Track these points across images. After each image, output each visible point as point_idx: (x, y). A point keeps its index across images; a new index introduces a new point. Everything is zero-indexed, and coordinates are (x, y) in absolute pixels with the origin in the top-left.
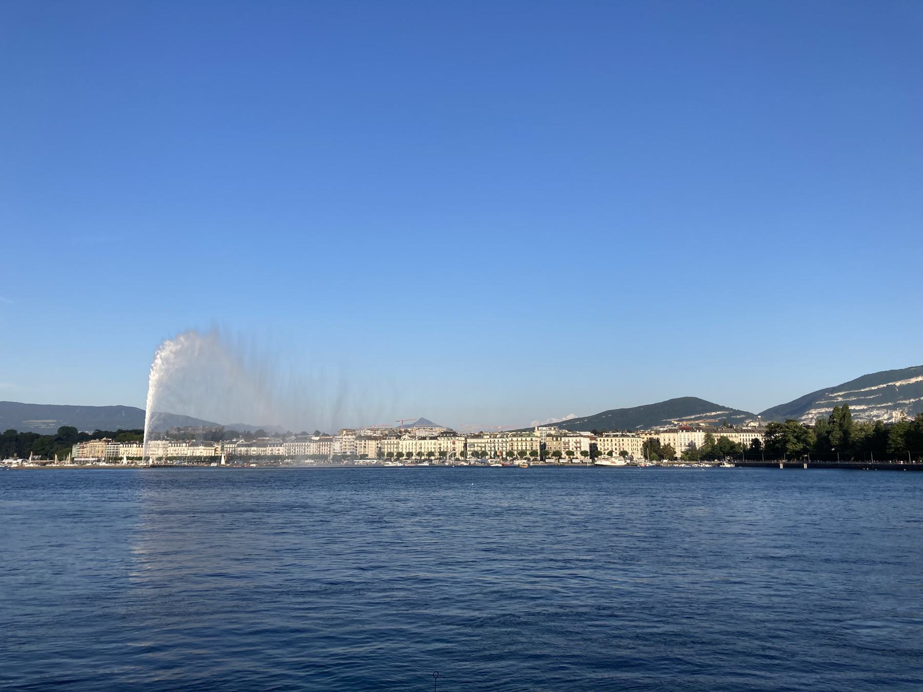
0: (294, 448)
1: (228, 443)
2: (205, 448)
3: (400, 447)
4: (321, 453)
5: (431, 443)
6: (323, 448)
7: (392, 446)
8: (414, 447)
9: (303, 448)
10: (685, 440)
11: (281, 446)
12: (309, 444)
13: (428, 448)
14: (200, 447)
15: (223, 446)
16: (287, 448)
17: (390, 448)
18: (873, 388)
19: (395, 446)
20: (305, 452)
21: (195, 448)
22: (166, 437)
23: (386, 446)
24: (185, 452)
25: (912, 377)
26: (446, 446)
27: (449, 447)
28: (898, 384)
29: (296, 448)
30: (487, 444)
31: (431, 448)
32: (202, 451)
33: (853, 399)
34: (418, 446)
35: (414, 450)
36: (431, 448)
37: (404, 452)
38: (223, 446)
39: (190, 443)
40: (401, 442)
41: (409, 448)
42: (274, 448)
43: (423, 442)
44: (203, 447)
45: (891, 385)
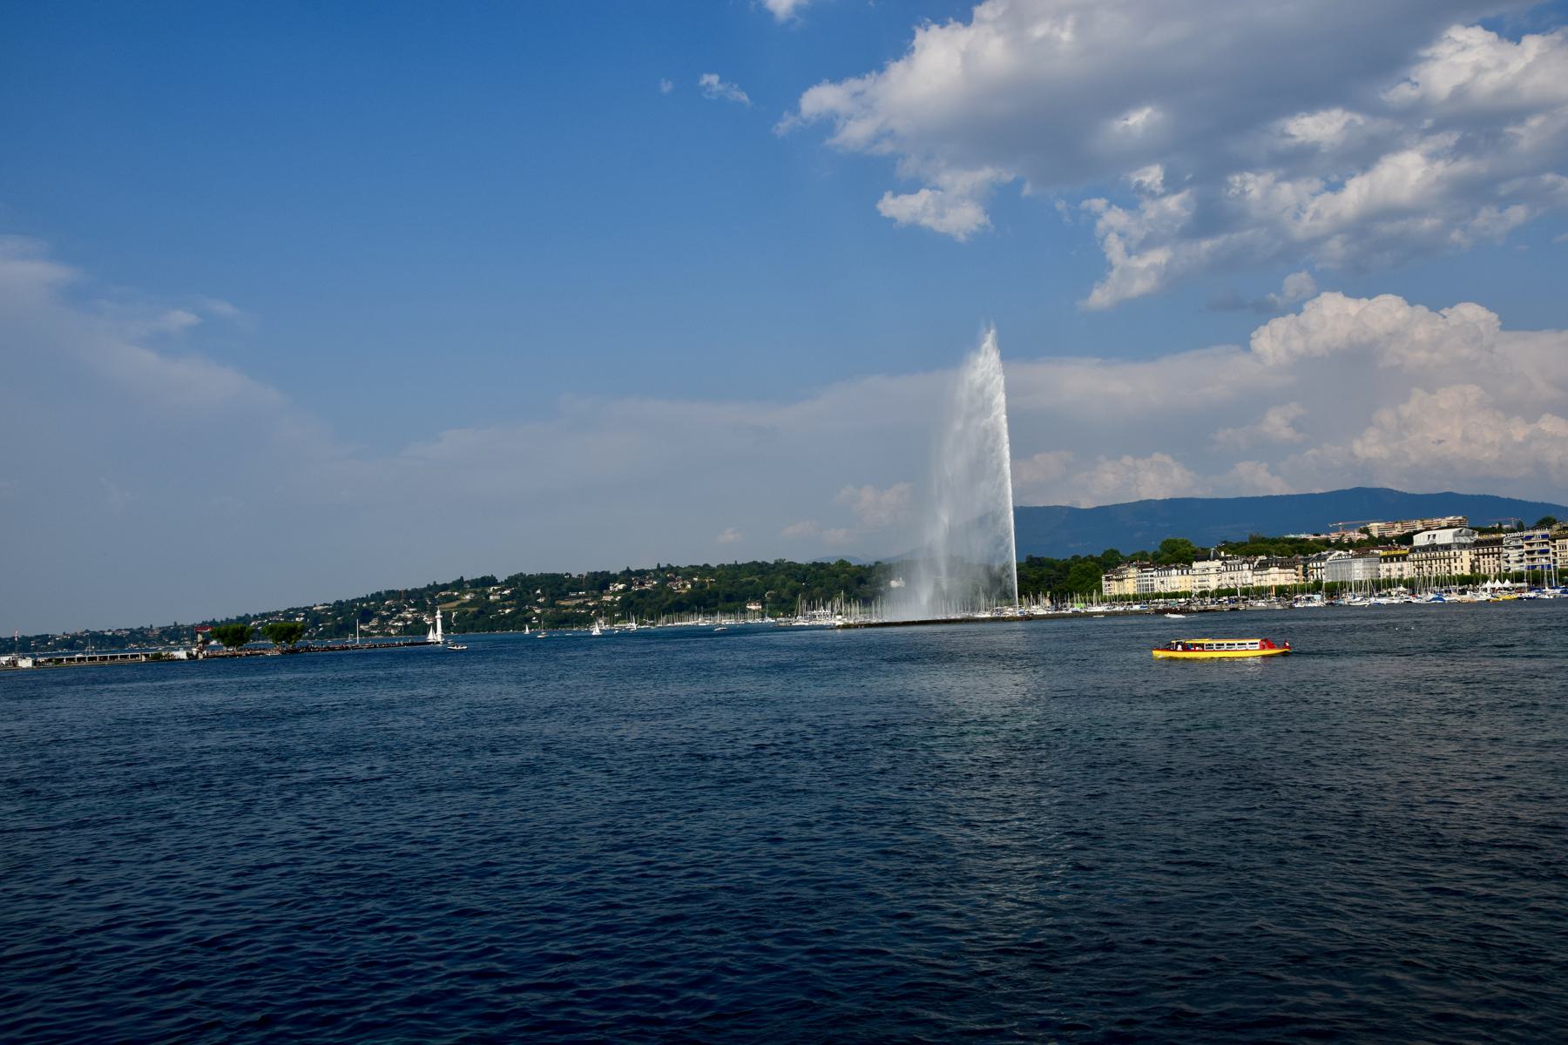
1: (1314, 560)
2: (1282, 570)
4: (1482, 571)
6: (1486, 559)
9: (1447, 561)
11: (1404, 560)
12: (1458, 553)
14: (1271, 570)
15: (1305, 566)
20: (1450, 572)
21: (1265, 572)
22: (1223, 554)
24: (1249, 581)
32: (1277, 576)
38: (1305, 566)
39: (1256, 563)
44: (1277, 569)
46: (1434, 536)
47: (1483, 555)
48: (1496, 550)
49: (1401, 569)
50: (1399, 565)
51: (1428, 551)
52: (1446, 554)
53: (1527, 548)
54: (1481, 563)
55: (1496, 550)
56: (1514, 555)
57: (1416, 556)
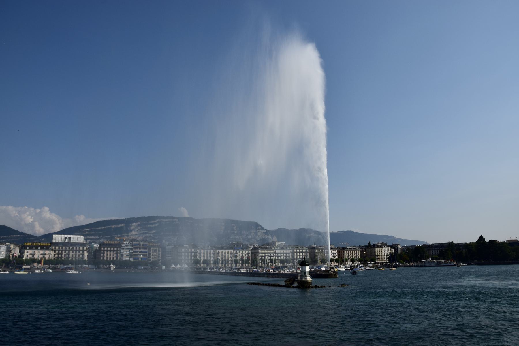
4: (105, 258)
5: (228, 252)
6: (109, 253)
7: (190, 254)
8: (212, 255)
9: (81, 252)
10: (384, 252)
13: (225, 257)
16: (57, 252)
18: (102, 228)
19: (193, 254)
23: (183, 254)
25: (119, 224)
26: (241, 255)
27: (244, 255)
28: (113, 227)
29: (71, 252)
31: (228, 257)
33: (93, 233)
34: (216, 255)
35: (220, 258)
36: (228, 257)
37: (220, 258)
40: (198, 251)
41: (207, 257)
42: (36, 252)
43: (220, 251)
45: (110, 227)
46: (70, 238)
47: (107, 251)
48: (116, 249)
49: (45, 254)
50: (41, 252)
51: (67, 246)
52: (81, 248)
53: (134, 250)
54: (105, 255)
55: (116, 249)
56: (126, 252)
57: (57, 248)
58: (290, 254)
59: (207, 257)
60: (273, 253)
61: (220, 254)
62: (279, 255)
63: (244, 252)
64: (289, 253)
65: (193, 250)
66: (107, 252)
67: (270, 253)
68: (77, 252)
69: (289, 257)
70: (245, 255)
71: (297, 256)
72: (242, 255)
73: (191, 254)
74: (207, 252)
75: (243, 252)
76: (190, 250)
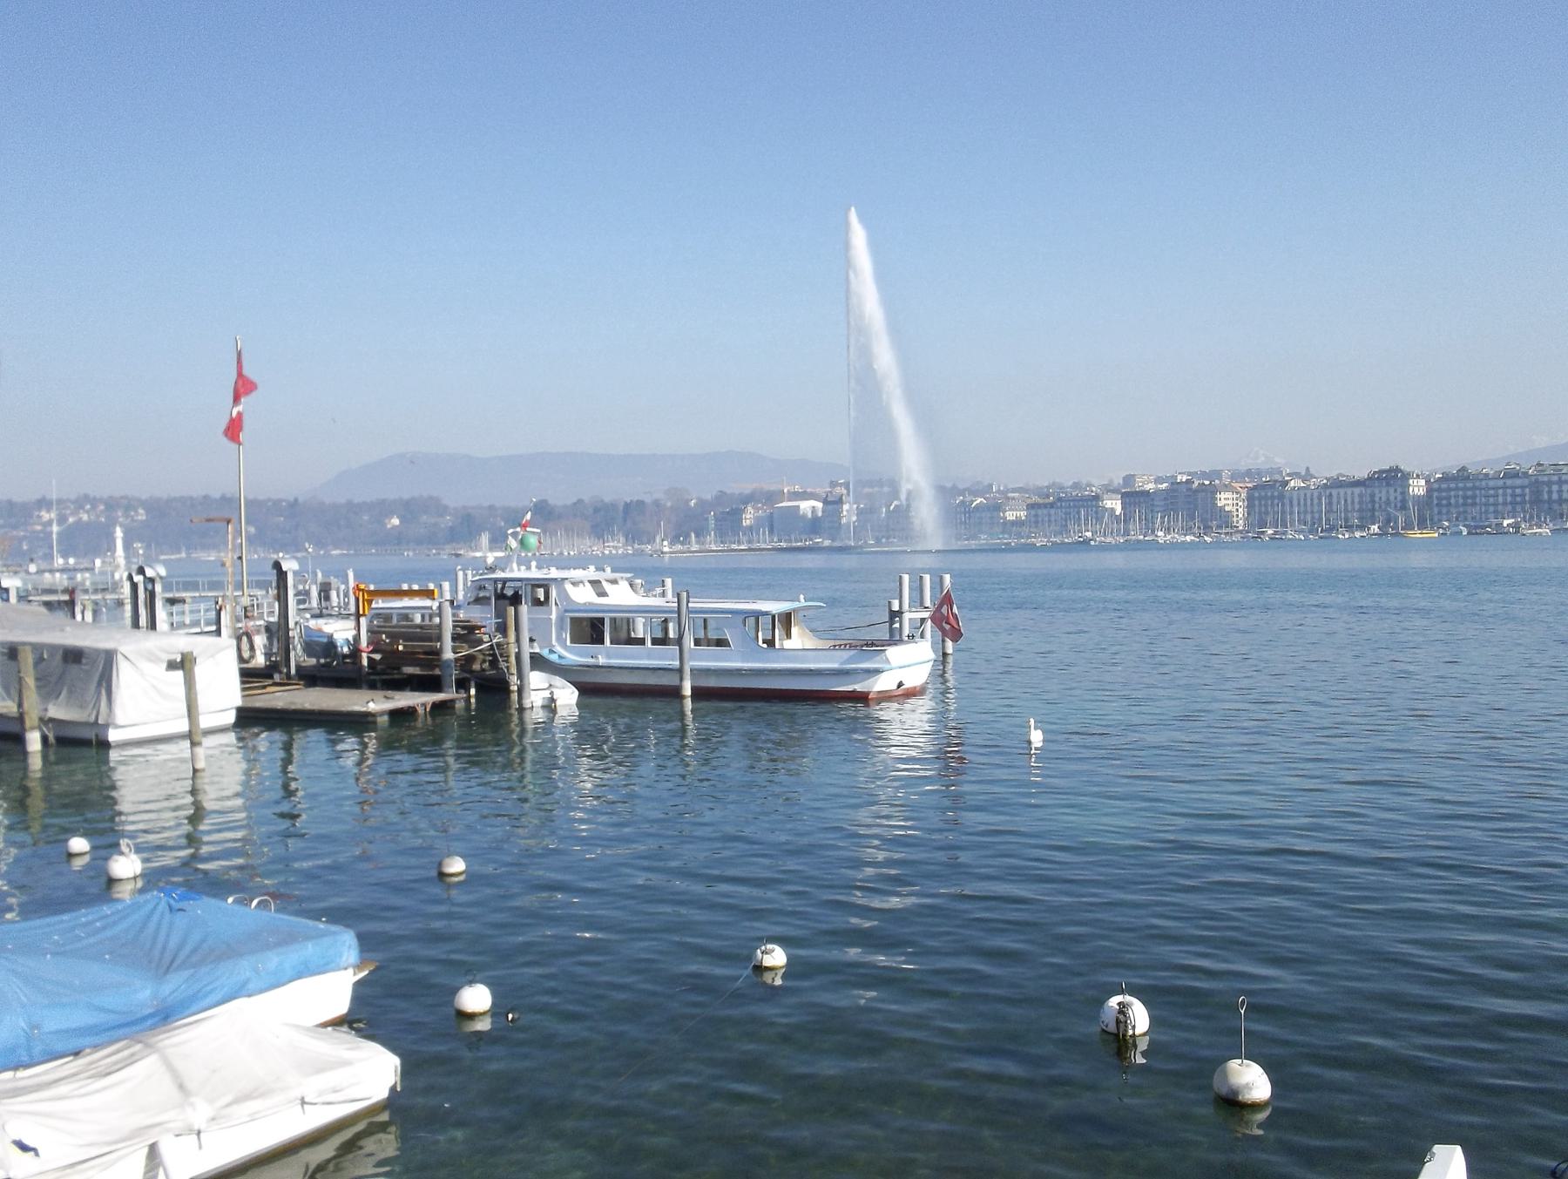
0: (1076, 510)
3: (1287, 501)
7: (1270, 502)
17: (1266, 506)
23: (1257, 502)
26: (1383, 499)
27: (1392, 498)
30: (1478, 492)
39: (892, 508)
40: (1287, 494)
42: (1040, 512)
43: (1334, 492)
50: (1045, 511)
58: (1527, 490)
59: (1305, 505)
60: (1474, 488)
61: (1335, 500)
62: (1492, 492)
63: (1392, 490)
64: (1523, 487)
65: (1276, 494)
66: (1130, 506)
67: (1465, 489)
68: (1090, 510)
69: (1523, 495)
70: (1396, 498)
71: (1550, 492)
72: (1388, 499)
73: (1272, 503)
74: (1305, 495)
75: (1388, 492)
76: (1269, 494)
